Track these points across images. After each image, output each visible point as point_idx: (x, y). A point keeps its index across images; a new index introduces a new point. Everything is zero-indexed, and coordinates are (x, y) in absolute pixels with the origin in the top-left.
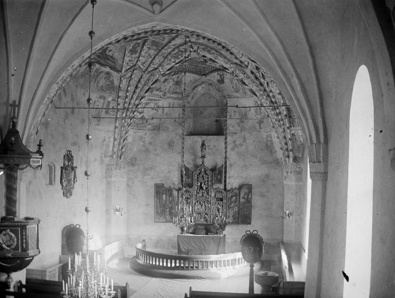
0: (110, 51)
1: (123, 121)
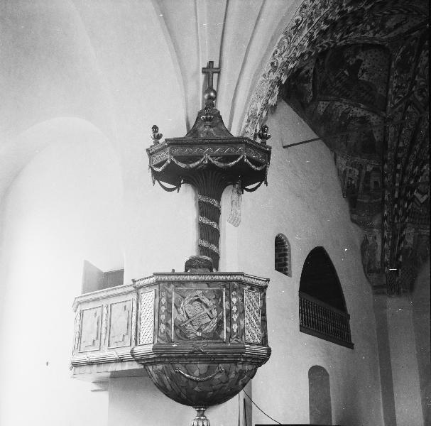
0: (364, 71)
1: (396, 206)
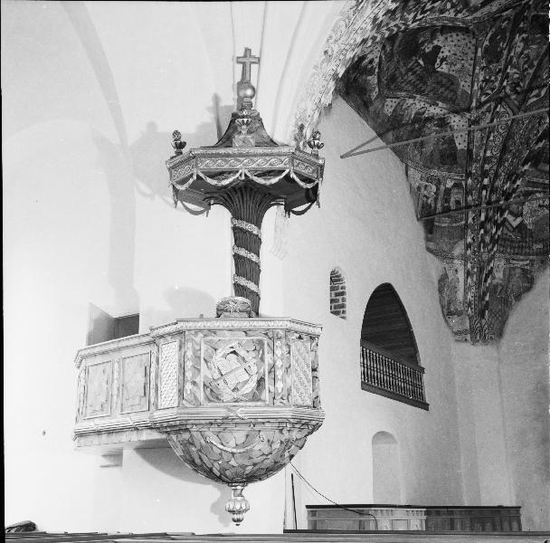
0: (443, 60)
1: (482, 231)
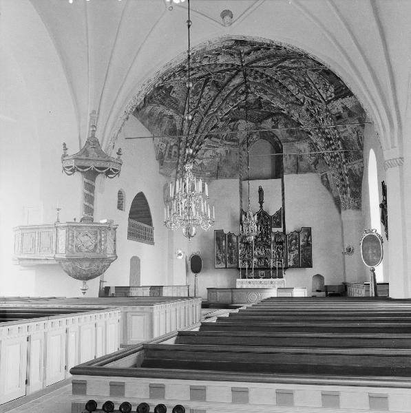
0: (174, 92)
